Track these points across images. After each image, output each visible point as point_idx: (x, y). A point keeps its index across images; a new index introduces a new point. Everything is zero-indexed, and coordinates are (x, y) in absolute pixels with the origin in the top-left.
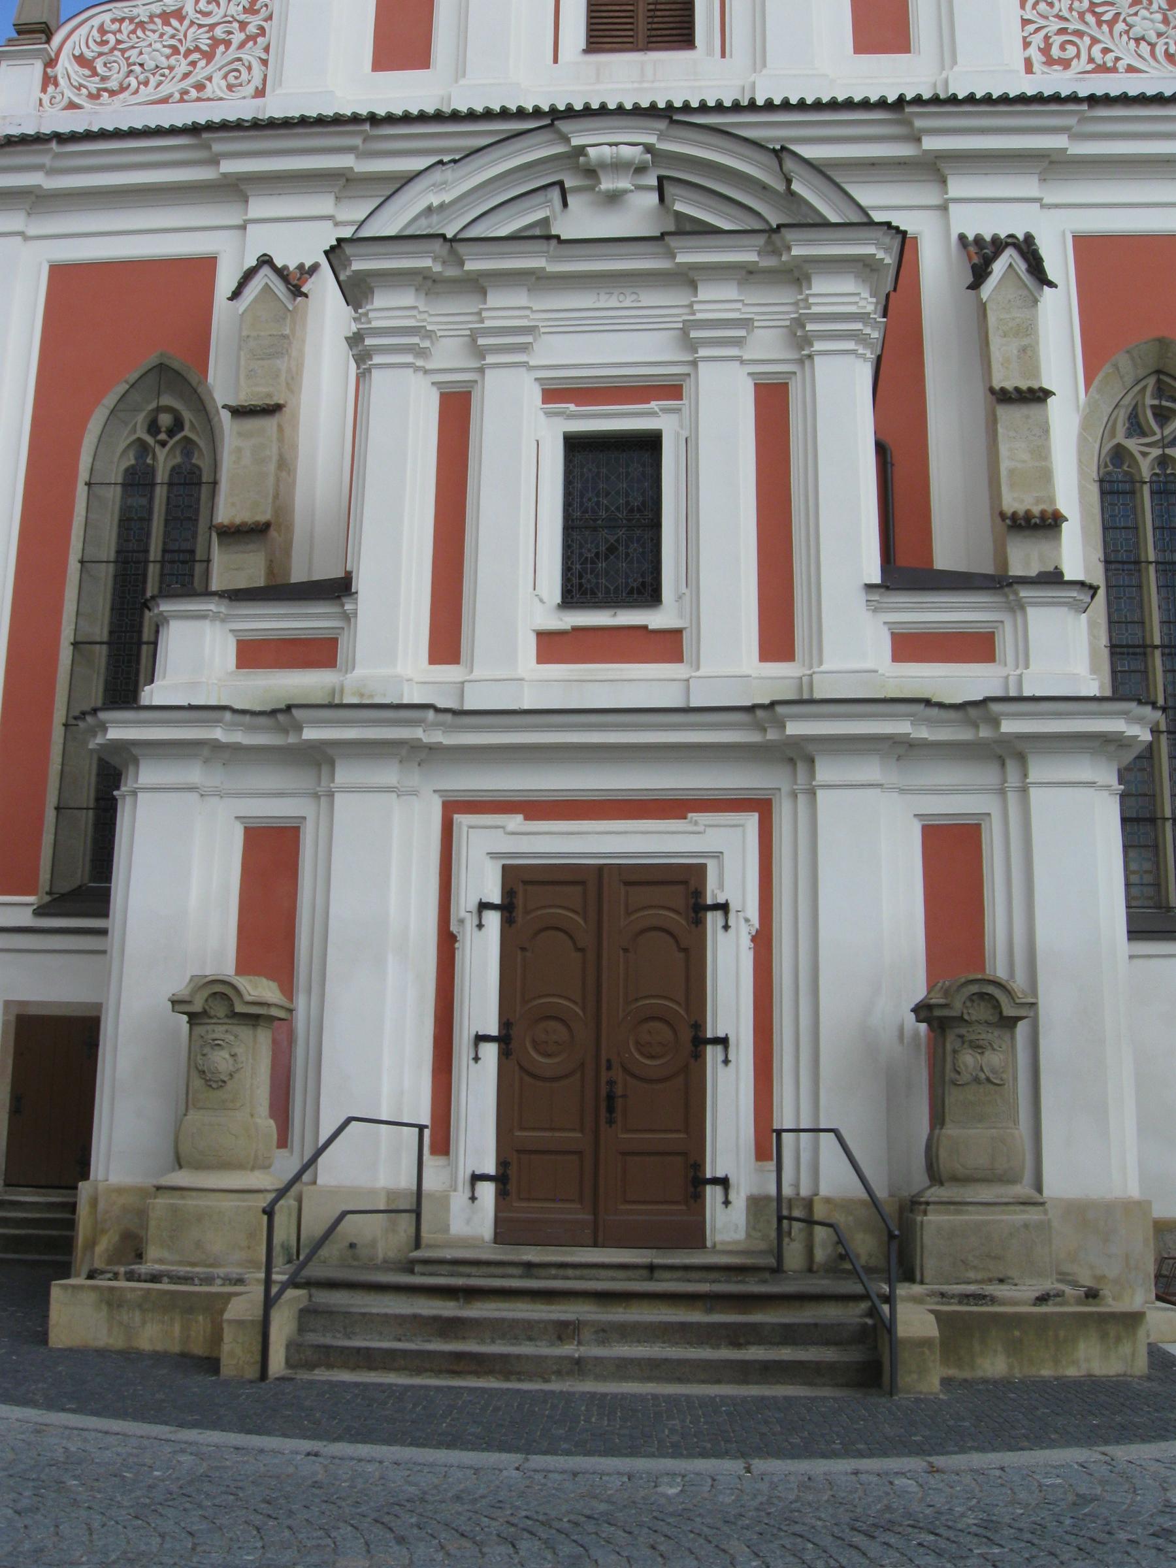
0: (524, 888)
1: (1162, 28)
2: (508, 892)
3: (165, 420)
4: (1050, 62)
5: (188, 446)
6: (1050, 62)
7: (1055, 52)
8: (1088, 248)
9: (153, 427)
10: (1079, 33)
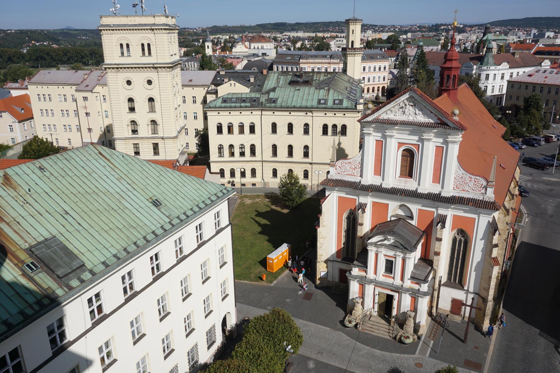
8: (455, 216)
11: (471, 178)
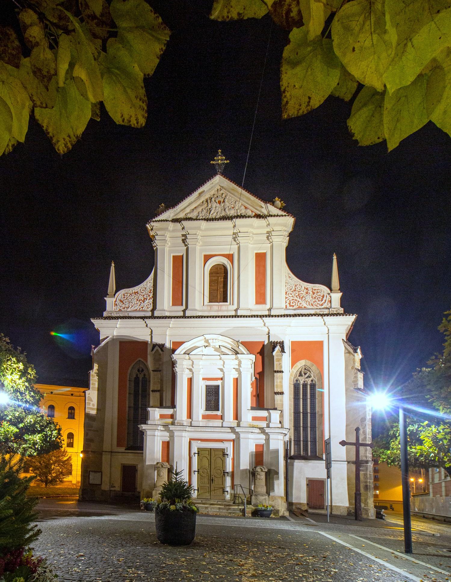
0: (200, 451)
1: (311, 299)
2: (199, 452)
3: (141, 369)
4: (290, 306)
5: (145, 375)
6: (290, 306)
7: (291, 304)
9: (139, 370)
10: (296, 300)
11: (307, 289)
